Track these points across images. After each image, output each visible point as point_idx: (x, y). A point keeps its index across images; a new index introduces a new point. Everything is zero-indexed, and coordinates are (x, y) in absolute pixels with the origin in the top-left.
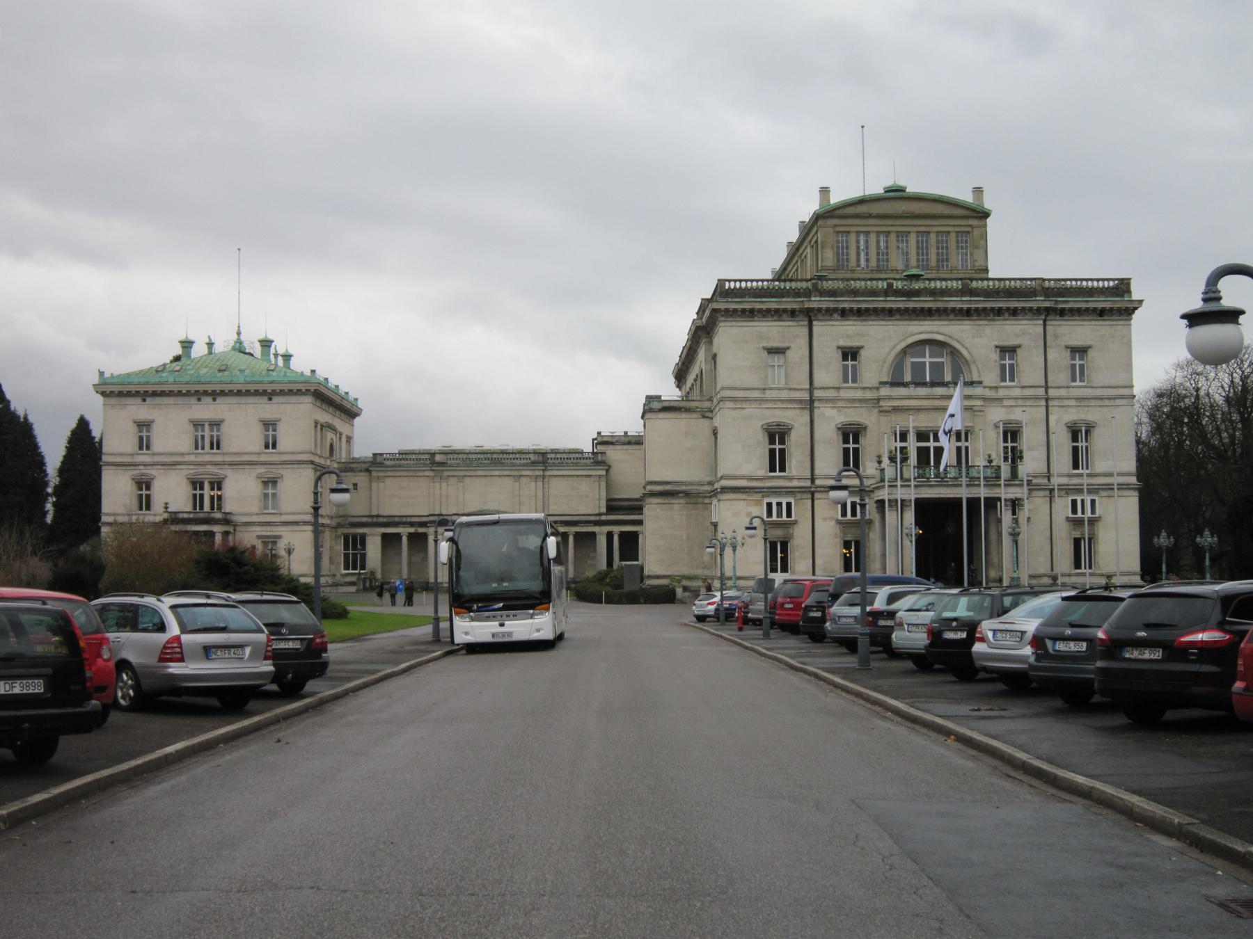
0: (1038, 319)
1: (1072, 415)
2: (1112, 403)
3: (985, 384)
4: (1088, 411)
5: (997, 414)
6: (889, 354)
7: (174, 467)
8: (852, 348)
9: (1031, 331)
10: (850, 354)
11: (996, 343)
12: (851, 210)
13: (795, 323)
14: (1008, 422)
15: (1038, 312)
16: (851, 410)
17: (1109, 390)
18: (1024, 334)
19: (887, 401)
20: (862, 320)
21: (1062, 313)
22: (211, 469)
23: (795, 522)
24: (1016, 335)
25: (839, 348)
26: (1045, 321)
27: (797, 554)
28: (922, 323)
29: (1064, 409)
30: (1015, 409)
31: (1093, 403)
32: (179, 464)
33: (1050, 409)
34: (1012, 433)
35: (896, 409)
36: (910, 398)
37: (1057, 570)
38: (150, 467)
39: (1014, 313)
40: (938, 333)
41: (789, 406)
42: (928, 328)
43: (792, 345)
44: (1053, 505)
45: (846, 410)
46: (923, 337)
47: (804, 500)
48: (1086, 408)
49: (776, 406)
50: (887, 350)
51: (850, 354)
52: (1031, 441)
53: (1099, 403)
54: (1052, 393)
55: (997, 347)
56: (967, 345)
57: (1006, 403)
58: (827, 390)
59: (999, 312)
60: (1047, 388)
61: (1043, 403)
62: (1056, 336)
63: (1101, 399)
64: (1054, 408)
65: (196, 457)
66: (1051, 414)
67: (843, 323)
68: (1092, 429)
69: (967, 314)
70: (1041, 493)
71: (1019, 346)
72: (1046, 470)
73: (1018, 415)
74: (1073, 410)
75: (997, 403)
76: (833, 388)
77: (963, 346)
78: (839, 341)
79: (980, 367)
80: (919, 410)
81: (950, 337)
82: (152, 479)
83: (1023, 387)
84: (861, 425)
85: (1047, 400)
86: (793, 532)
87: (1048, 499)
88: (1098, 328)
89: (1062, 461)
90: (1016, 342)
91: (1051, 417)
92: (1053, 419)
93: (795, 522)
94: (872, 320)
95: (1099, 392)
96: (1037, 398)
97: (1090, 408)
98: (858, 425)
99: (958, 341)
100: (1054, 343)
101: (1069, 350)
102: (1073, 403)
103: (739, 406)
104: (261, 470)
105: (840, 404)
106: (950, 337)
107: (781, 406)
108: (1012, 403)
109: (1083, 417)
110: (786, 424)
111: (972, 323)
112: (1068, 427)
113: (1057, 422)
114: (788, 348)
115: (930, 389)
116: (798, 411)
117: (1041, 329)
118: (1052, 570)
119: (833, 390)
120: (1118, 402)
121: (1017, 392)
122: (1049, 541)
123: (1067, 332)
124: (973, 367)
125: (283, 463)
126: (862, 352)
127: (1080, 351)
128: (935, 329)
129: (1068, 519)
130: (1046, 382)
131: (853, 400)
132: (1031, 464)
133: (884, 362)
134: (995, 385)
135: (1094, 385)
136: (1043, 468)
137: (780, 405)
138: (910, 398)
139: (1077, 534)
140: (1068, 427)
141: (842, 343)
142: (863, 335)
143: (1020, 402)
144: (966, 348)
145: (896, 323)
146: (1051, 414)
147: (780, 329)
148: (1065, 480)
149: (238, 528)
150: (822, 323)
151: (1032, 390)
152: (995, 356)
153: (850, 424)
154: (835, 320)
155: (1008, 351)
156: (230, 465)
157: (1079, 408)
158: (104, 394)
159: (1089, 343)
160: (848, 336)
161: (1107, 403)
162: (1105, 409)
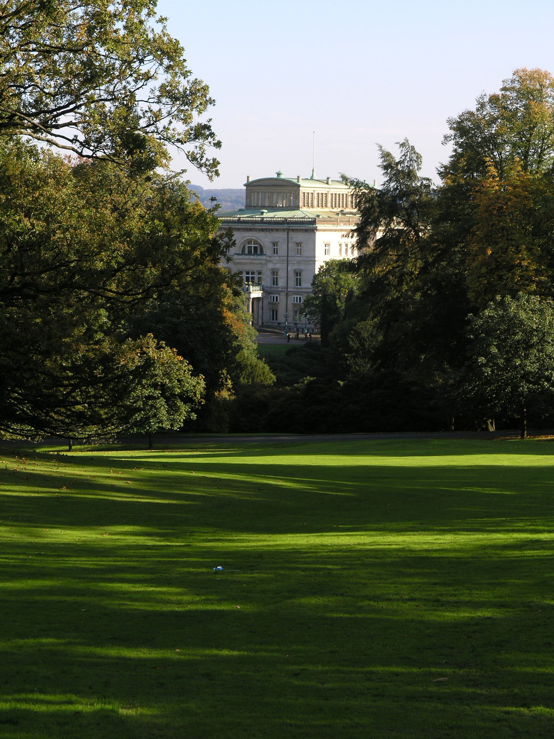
5: (271, 266)
12: (256, 184)
15: (284, 230)
21: (293, 230)
34: (274, 272)
35: (238, 263)
36: (242, 259)
42: (250, 235)
52: (282, 274)
59: (272, 230)
61: (286, 262)
62: (291, 238)
72: (286, 286)
73: (278, 266)
80: (245, 264)
87: (285, 296)
89: (292, 283)
92: (289, 267)
95: (305, 259)
117: (286, 236)
121: (277, 258)
127: (298, 244)
132: (282, 283)
138: (242, 259)
148: (292, 290)
155: (275, 244)
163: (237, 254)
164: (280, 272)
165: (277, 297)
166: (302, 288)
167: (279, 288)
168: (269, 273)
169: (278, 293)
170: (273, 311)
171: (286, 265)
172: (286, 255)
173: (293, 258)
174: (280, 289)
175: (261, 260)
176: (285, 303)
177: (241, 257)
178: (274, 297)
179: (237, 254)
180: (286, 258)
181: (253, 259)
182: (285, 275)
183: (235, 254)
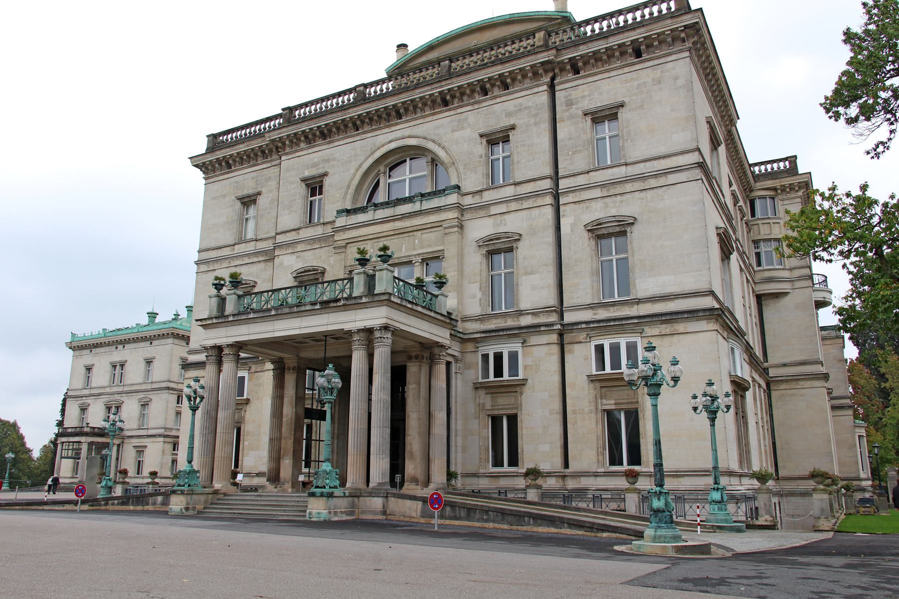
0: (538, 86)
1: (598, 211)
2: (662, 181)
3: (464, 190)
4: (622, 201)
6: (355, 175)
7: (99, 397)
8: (314, 178)
9: (530, 104)
10: (315, 186)
11: (482, 131)
13: (269, 165)
14: (492, 237)
16: (310, 253)
17: (655, 163)
18: (520, 110)
19: (341, 233)
20: (330, 142)
22: (117, 397)
23: (248, 401)
24: (509, 115)
25: (304, 180)
26: (552, 87)
27: (246, 443)
28: (393, 129)
29: (583, 205)
30: (506, 217)
31: (629, 187)
32: (100, 395)
33: (562, 208)
37: (574, 466)
38: (88, 398)
39: (505, 84)
40: (410, 137)
41: (255, 259)
42: (398, 134)
43: (264, 190)
44: (568, 357)
45: (304, 253)
46: (393, 146)
47: (258, 374)
48: (619, 197)
49: (243, 263)
50: (353, 171)
51: (315, 186)
53: (638, 185)
54: (563, 184)
55: (481, 136)
56: (446, 144)
57: (494, 210)
58: (288, 234)
60: (556, 177)
61: (549, 200)
63: (642, 178)
64: (567, 208)
65: (110, 389)
66: (564, 215)
67: (310, 151)
68: (628, 230)
69: (445, 101)
70: (545, 339)
71: (513, 128)
73: (512, 223)
74: (598, 205)
75: (482, 213)
76: (294, 230)
77: (439, 145)
78: (304, 173)
79: (461, 168)
81: (425, 138)
82: (88, 406)
83: (516, 184)
84: (317, 270)
85: (556, 196)
86: (245, 414)
87: (556, 349)
88: (634, 75)
90: (506, 122)
91: (563, 221)
93: (248, 401)
94: (338, 140)
96: (537, 195)
97: (625, 197)
98: (314, 270)
99: (433, 141)
100: (567, 114)
101: (589, 119)
102: (597, 193)
103: (211, 268)
104: (141, 395)
105: (300, 247)
106: (425, 138)
107: (247, 261)
108: (502, 208)
109: (614, 212)
110: (248, 282)
111: (452, 113)
112: (589, 230)
113: (573, 226)
114: (259, 194)
115: (393, 209)
116: (263, 264)
117: (544, 98)
118: (566, 465)
119: (294, 232)
120: (672, 179)
121: (509, 191)
122: (559, 418)
123: (586, 93)
124: (452, 171)
125: (153, 390)
126: (327, 182)
128: (407, 132)
129: (592, 379)
130: (557, 172)
131: (312, 240)
133: (348, 187)
134: (479, 189)
135: (629, 161)
136: (551, 299)
137: (247, 261)
139: (609, 404)
140: (589, 230)
141: (307, 174)
142: (327, 161)
143: (513, 206)
144: (443, 148)
145: (364, 136)
146: (564, 215)
147: (254, 174)
149: (126, 441)
150: (290, 157)
151: (532, 184)
152: (480, 148)
153: (305, 271)
154: (302, 150)
156: (126, 393)
157: (607, 200)
158: (73, 348)
159: (620, 99)
160: (314, 165)
161: (653, 183)
162: (649, 194)
163: (348, 212)
164: (523, 250)
165: (513, 356)
166: (639, 301)
167: (520, 313)
168: (475, 260)
169: (522, 333)
170: (496, 421)
171: (549, 212)
172: (548, 171)
173: (581, 180)
174: (526, 321)
175: (439, 209)
176: (557, 378)
177: (361, 218)
178: (498, 357)
179: (348, 212)
180: (547, 184)
181: (403, 217)
182: (549, 253)
183: (340, 212)
